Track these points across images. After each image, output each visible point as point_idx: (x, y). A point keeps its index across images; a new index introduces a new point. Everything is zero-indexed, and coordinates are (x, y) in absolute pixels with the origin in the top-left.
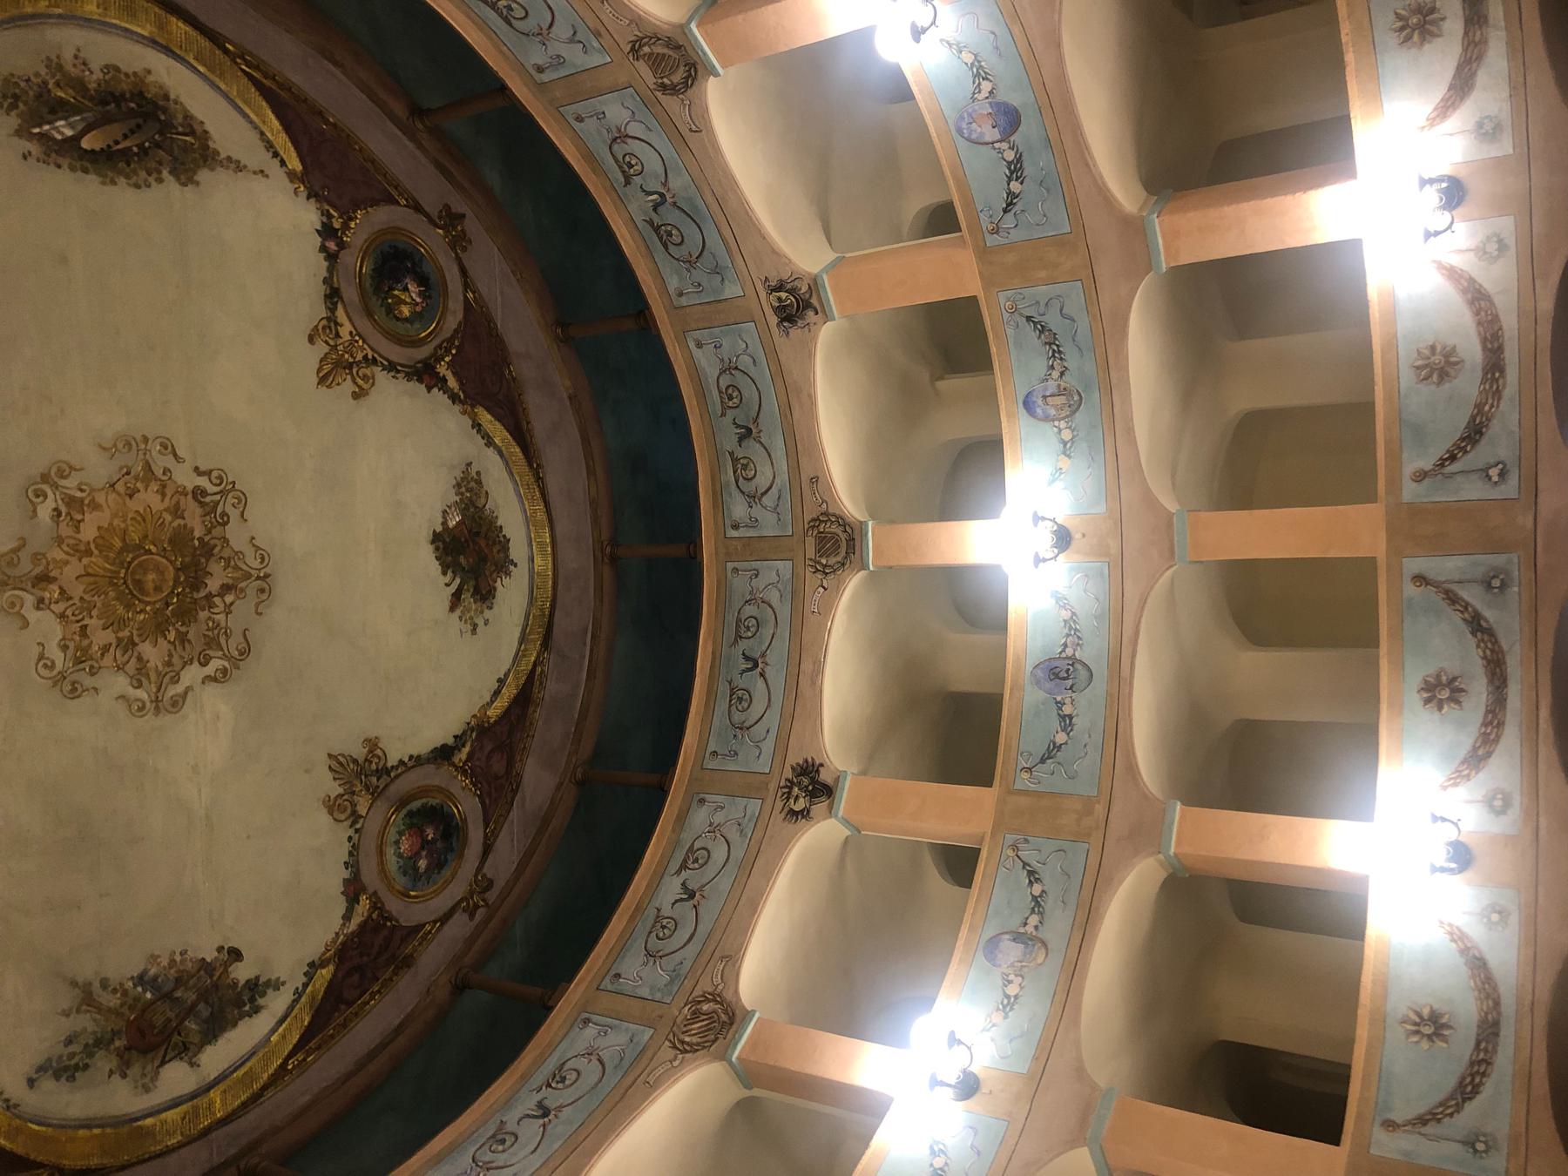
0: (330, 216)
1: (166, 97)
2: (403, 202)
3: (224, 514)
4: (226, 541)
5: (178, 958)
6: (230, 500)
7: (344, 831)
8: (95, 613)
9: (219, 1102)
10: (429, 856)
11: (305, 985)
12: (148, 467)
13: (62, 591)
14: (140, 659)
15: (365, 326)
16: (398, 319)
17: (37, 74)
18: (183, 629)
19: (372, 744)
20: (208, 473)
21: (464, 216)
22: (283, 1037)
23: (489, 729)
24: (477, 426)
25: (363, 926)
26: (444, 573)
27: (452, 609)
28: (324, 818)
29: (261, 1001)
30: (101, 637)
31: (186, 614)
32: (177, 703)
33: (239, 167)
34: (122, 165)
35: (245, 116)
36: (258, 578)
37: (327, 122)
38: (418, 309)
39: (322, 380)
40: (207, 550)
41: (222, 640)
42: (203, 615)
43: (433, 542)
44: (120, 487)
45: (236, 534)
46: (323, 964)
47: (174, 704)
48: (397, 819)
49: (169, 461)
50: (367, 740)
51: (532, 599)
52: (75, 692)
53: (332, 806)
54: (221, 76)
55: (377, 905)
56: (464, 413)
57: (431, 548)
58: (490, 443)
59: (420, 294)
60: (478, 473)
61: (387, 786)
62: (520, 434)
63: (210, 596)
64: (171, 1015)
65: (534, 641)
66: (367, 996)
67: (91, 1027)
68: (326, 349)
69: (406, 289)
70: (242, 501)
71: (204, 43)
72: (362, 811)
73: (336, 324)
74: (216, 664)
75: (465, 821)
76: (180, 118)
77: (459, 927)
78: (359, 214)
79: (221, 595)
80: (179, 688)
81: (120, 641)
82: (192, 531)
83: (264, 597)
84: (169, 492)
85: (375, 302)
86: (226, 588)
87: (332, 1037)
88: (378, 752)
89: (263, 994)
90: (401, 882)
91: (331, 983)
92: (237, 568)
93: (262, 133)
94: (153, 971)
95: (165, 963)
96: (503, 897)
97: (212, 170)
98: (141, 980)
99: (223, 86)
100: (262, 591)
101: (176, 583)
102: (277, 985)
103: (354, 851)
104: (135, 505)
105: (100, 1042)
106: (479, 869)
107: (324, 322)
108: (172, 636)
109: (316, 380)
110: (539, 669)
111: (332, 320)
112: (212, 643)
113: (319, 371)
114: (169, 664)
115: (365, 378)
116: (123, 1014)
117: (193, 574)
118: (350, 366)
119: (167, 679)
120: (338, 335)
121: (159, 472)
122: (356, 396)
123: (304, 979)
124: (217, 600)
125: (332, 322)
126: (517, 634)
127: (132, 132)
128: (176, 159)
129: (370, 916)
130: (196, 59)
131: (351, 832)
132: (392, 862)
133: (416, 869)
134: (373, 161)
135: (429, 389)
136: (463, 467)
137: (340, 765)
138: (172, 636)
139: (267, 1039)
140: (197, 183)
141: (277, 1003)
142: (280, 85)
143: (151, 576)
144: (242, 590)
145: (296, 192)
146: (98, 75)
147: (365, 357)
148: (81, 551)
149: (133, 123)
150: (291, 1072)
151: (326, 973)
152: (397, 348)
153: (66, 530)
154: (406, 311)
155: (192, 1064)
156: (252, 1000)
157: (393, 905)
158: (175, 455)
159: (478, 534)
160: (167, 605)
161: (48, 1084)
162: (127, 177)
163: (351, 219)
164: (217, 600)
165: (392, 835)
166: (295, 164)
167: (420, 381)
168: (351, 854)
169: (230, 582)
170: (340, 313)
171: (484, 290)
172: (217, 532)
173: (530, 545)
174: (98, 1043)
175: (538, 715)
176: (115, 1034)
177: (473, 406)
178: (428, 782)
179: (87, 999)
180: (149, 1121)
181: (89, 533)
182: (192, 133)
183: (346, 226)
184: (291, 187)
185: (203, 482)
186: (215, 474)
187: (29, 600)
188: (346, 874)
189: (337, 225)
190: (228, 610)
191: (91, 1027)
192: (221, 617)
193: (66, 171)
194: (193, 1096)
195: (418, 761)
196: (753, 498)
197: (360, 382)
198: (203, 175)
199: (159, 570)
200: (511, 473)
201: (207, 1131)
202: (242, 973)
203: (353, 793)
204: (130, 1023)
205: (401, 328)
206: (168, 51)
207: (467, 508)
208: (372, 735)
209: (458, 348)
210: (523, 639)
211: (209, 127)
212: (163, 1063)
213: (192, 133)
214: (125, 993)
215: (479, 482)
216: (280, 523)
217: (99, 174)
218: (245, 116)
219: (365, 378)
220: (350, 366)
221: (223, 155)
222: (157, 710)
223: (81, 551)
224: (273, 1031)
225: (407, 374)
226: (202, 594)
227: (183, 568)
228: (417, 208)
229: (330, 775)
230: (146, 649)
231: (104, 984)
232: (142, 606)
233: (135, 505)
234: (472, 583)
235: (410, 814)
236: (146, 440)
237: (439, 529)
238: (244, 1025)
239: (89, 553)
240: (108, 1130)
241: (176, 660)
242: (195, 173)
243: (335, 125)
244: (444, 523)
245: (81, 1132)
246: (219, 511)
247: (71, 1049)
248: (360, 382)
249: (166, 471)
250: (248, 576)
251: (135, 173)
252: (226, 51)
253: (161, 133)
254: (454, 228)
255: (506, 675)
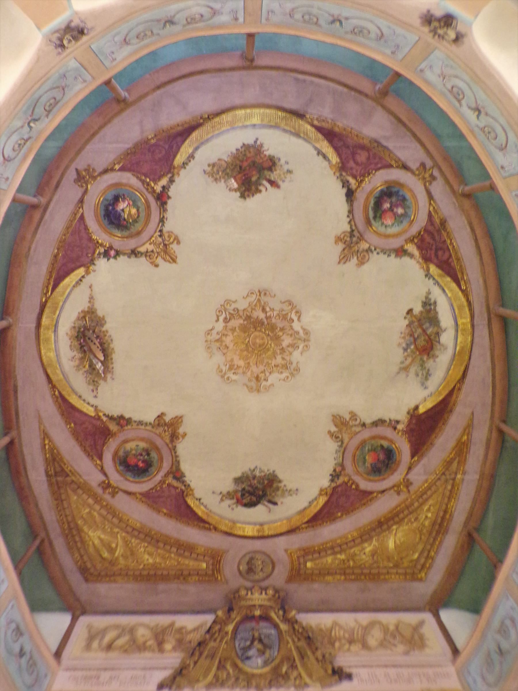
0: (99, 254)
1: (74, 327)
2: (81, 209)
3: (234, 310)
4: (244, 310)
5: (403, 335)
6: (228, 307)
7: (374, 257)
8: (270, 362)
9: (465, 320)
10: (397, 206)
11: (434, 279)
12: (217, 341)
13: (262, 372)
14: (288, 346)
15: (145, 236)
16: (138, 216)
17: (83, 374)
18: (279, 329)
19: (338, 239)
20: (218, 317)
21: (77, 170)
22: (451, 291)
23: (343, 163)
24: (184, 165)
25: (419, 248)
26: (260, 191)
27: (278, 187)
28: (366, 267)
29: (432, 301)
30: (279, 360)
31: (273, 328)
32: (307, 332)
33: (91, 298)
34: (106, 346)
35: (69, 294)
36: (260, 295)
37: (58, 254)
38: (131, 203)
39: (174, 260)
40: (248, 318)
41: (284, 313)
42: (274, 321)
43: (245, 198)
44: (225, 351)
45: (242, 305)
46: (428, 270)
47: (307, 334)
48: (376, 225)
49: (214, 332)
50: (336, 242)
51: (276, 127)
52: (297, 370)
53: (361, 263)
54: (57, 304)
55: (411, 240)
56: (178, 174)
57: (248, 199)
58: (191, 157)
59: (123, 201)
60: (209, 165)
61: (359, 232)
62: (186, 131)
63: (267, 318)
64: (423, 338)
65: (299, 126)
66: (450, 247)
67: (416, 368)
68: (159, 258)
69: (123, 210)
70: (228, 302)
71: (47, 311)
72: (366, 246)
73: (147, 252)
74: (294, 316)
75: (386, 182)
76: (80, 322)
77: (438, 188)
78: (94, 237)
79: (266, 313)
80: (301, 332)
81: (280, 353)
82: (241, 324)
83: (268, 293)
84: (226, 333)
85: (134, 229)
86: (264, 310)
87: (461, 266)
88: (342, 237)
89: (430, 300)
90: (405, 224)
91: (439, 266)
92: (256, 305)
93: (74, 286)
94: (404, 345)
95: (403, 341)
96: (432, 158)
97: (96, 310)
98: (405, 350)
99: (61, 304)
100: (265, 294)
101: (260, 331)
102: (429, 293)
103: (384, 251)
104: (231, 346)
105: (422, 365)
106: (413, 173)
107: (148, 258)
108: (281, 334)
109: (174, 265)
110: (316, 123)
111: (147, 254)
112: (284, 317)
113: (170, 262)
114: (291, 335)
115: (169, 237)
116: (415, 357)
117: (257, 324)
118: (165, 245)
119: (297, 336)
120: (152, 251)
121: (218, 337)
122: (179, 243)
123: (431, 279)
124: (268, 314)
125: (147, 254)
126: (294, 139)
127: (92, 341)
128: (97, 324)
129: (416, 244)
130: (55, 314)
131: (375, 253)
132: (395, 230)
133: (402, 215)
134: (67, 228)
135: (169, 197)
136: (207, 176)
137: (344, 259)
138: (281, 334)
139: (449, 299)
140: (103, 316)
141: (437, 294)
142: (51, 277)
143: (258, 341)
144: (265, 303)
145: (94, 271)
146: (75, 353)
147: (160, 236)
148: (248, 366)
149: (89, 341)
150: (467, 288)
151: (433, 269)
152: (153, 216)
153: (241, 371)
154: (134, 211)
155: (445, 330)
156: (430, 305)
157: (414, 230)
158: (212, 330)
159: (241, 167)
160: (269, 335)
161: (429, 383)
162: (109, 344)
163: (98, 242)
164: (268, 314)
165: (382, 229)
166: (81, 271)
167: (165, 203)
168: (385, 253)
169: (261, 309)
170: (142, 249)
171: (112, 157)
172: (241, 313)
173: (246, 127)
174: (422, 366)
175: (342, 124)
176: (421, 359)
177: (174, 168)
178: (362, 208)
179: (405, 369)
180: (458, 348)
181: (241, 363)
182: (84, 317)
183: (101, 245)
184: (92, 274)
185: (221, 319)
186: (218, 313)
187: (264, 383)
188: (393, 255)
189: (102, 250)
190: (272, 310)
191: (416, 368)
192: (275, 313)
193: (114, 365)
194: (457, 331)
195: (351, 212)
196: (215, 13)
197: (172, 240)
198: (100, 313)
199: (256, 337)
200: (207, 140)
201: (473, 326)
202: (418, 309)
203: (358, 251)
204: (420, 354)
205: (143, 214)
206: (56, 326)
207: (227, 174)
208: (333, 240)
209: (146, 176)
210: (297, 135)
211: (80, 311)
212: (439, 342)
213: (84, 317)
214: (408, 356)
215: (214, 165)
216: (237, 286)
217: (111, 354)
218: (69, 294)
219: (169, 237)
220: (165, 245)
221: (89, 305)
222: (308, 340)
223: (248, 366)
224: (446, 295)
225: (164, 211)
226: (265, 321)
227: (255, 328)
228: (81, 201)
229: (348, 264)
230: (285, 344)
231: (402, 363)
232: (269, 345)
233: (231, 346)
234: (267, 173)
235: (375, 218)
236: (206, 341)
237: (238, 194)
238: (438, 309)
239: (249, 363)
240: (454, 362)
241: (290, 332)
242: (100, 317)
243: (58, 249)
244: (236, 190)
245: (450, 372)
246: (232, 312)
247: (420, 374)
248: (172, 240)
249: (218, 333)
250: (259, 300)
251: (107, 341)
252: (46, 301)
253: (89, 330)
254: (84, 178)
255: (316, 148)
